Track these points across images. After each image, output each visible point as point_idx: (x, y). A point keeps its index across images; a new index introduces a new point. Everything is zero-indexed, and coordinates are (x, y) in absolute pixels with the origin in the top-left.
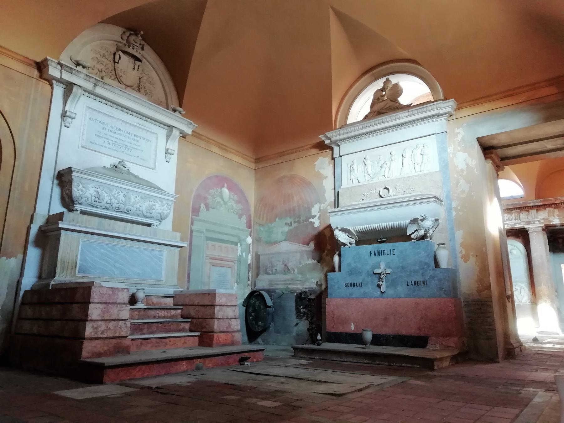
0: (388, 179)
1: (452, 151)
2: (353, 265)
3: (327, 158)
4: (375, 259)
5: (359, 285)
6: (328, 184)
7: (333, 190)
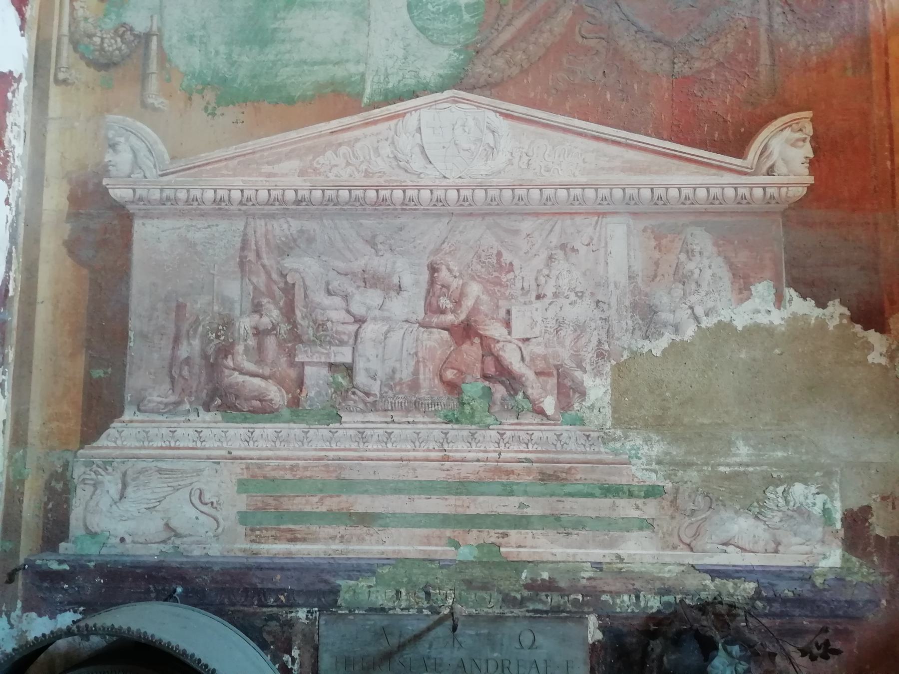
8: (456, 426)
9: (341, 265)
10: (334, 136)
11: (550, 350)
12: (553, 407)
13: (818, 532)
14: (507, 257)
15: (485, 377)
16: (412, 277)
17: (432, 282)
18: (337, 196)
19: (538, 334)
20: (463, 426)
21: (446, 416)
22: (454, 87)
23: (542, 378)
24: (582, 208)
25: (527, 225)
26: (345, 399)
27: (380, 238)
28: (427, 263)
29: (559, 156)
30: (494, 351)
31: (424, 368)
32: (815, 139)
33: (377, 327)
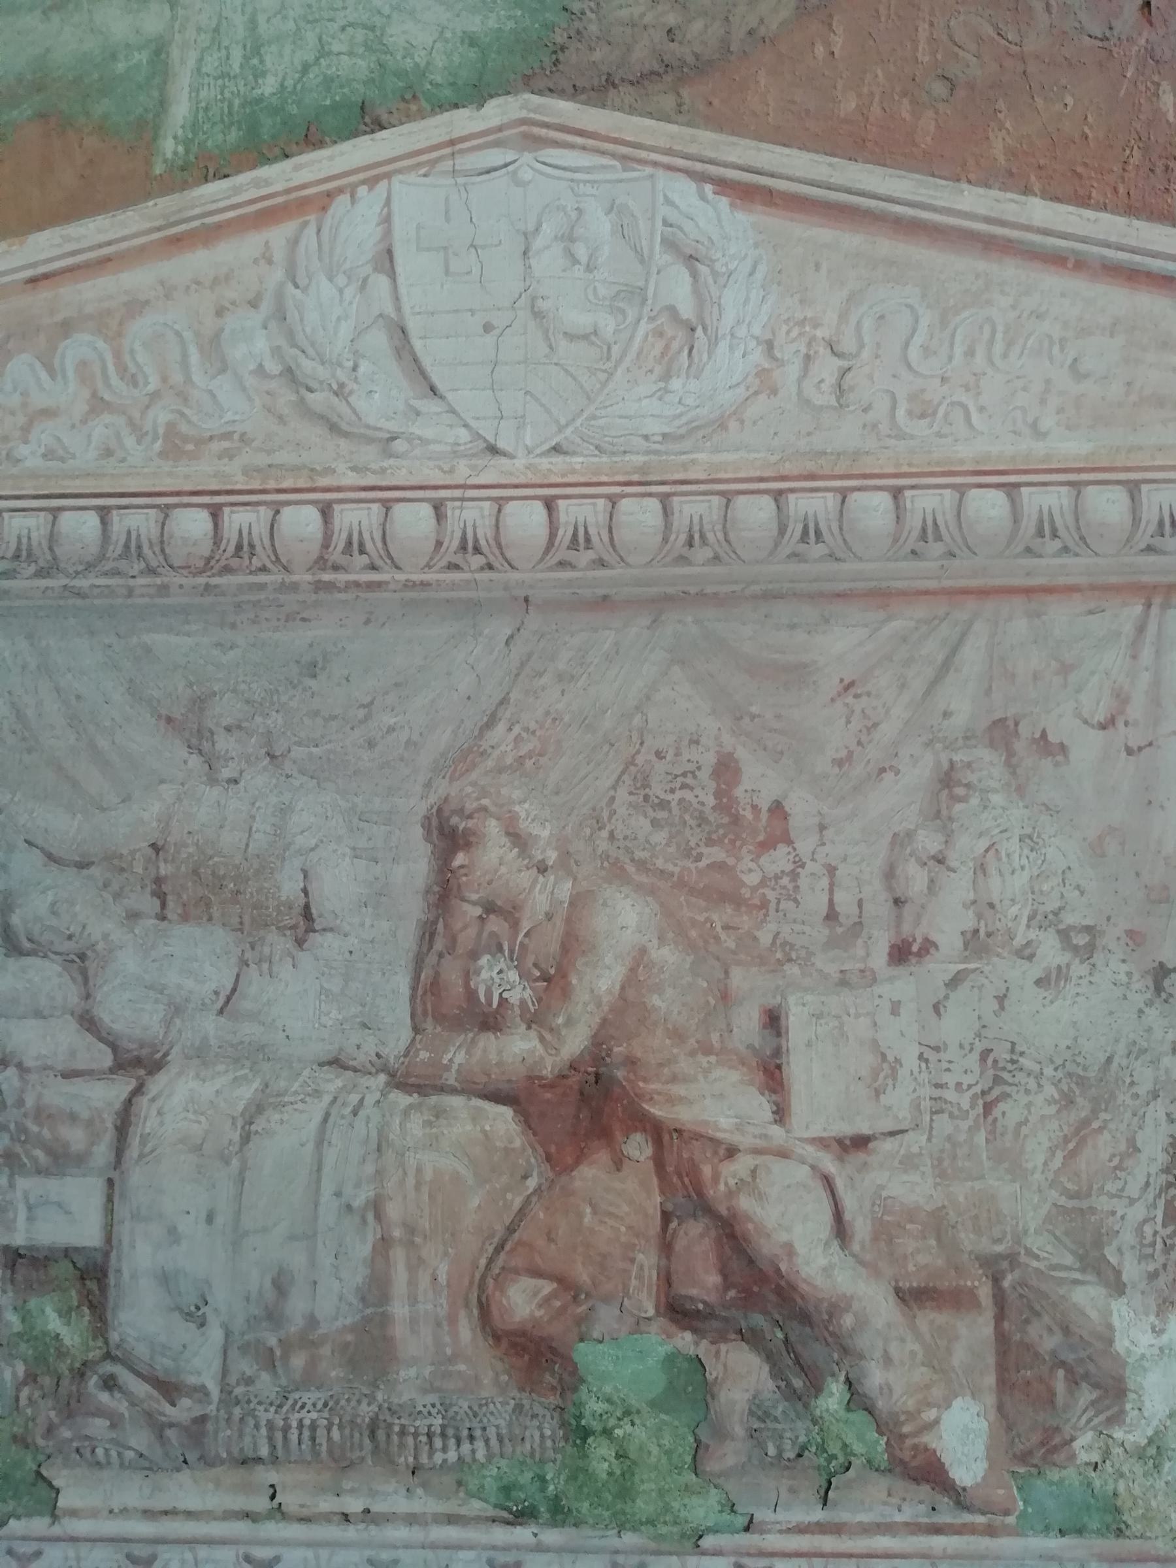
8: (551, 1536)
9: (62, 826)
10: (44, 294)
11: (961, 1191)
12: (980, 1448)
14: (760, 782)
15: (679, 1312)
16: (356, 870)
17: (444, 891)
18: (53, 538)
19: (904, 1115)
20: (587, 1536)
21: (507, 1490)
22: (528, 82)
23: (928, 1319)
24: (1076, 568)
25: (842, 643)
26: (72, 1407)
27: (226, 709)
28: (422, 808)
29: (970, 353)
30: (716, 1193)
31: (412, 1269)
33: (207, 1091)
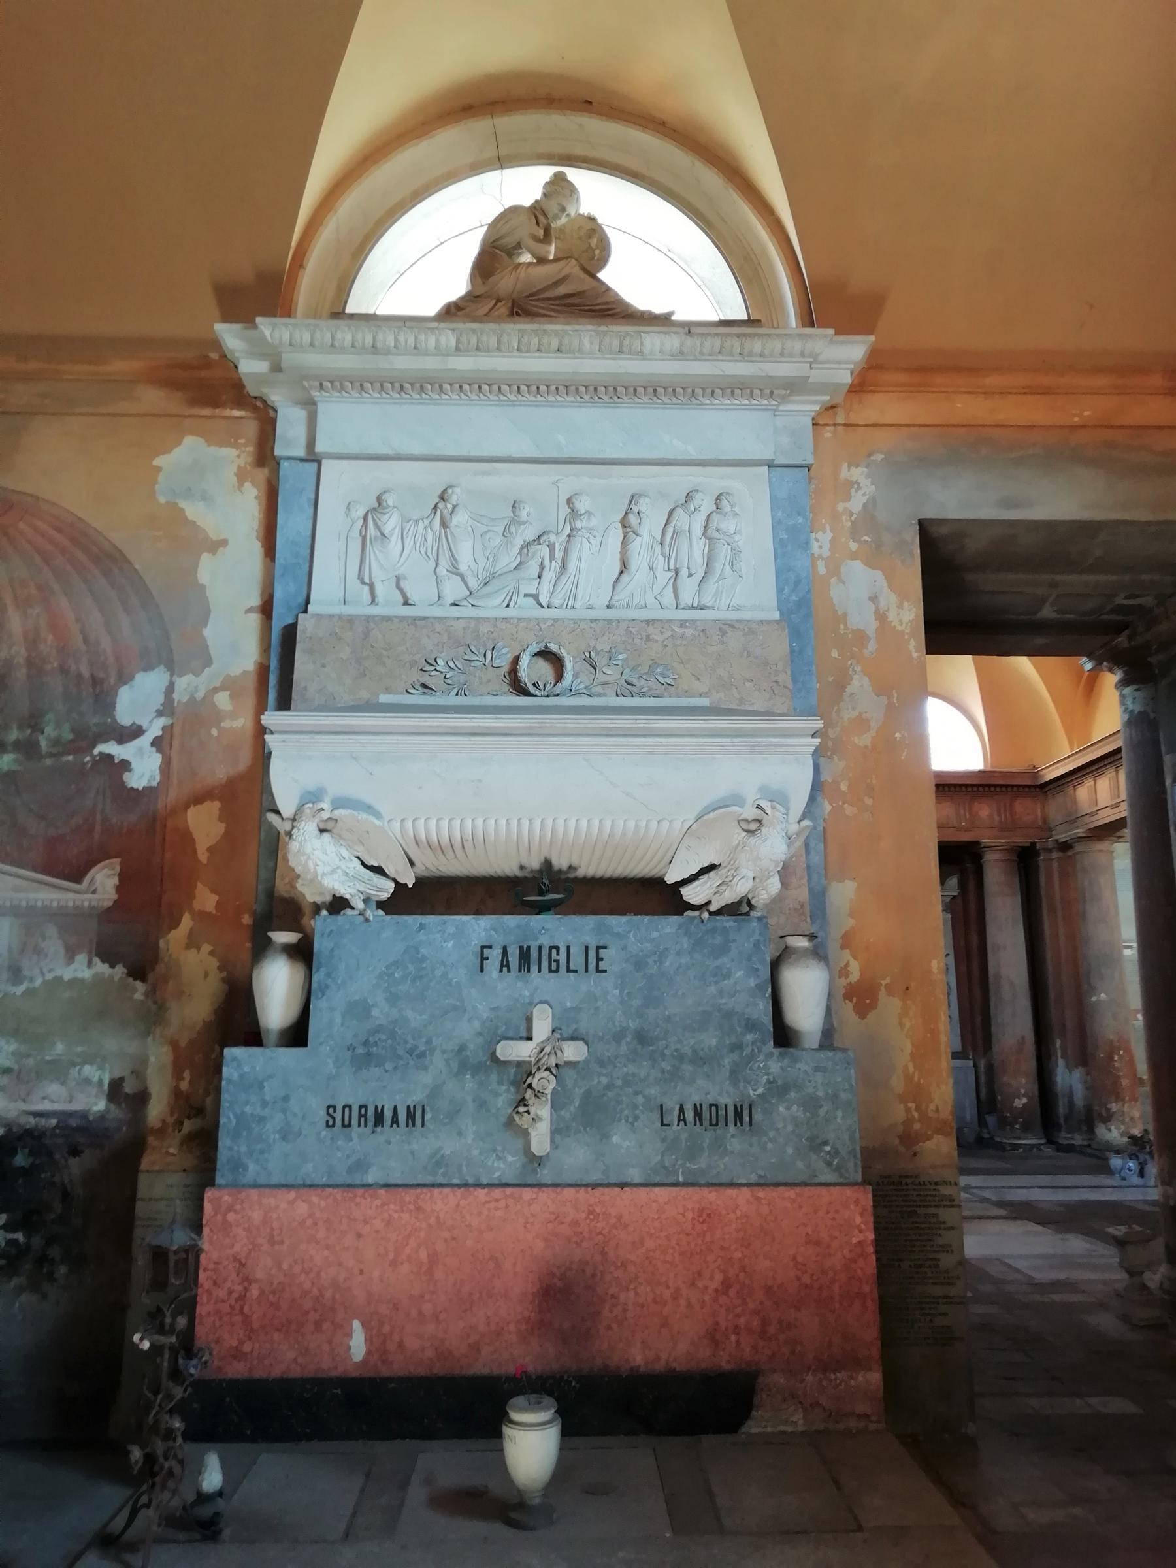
0: (552, 613)
1: (826, 553)
2: (381, 1013)
3: (230, 452)
4: (506, 988)
5: (411, 1115)
6: (229, 585)
7: (255, 619)
13: (95, 1091)
32: (120, 875)
